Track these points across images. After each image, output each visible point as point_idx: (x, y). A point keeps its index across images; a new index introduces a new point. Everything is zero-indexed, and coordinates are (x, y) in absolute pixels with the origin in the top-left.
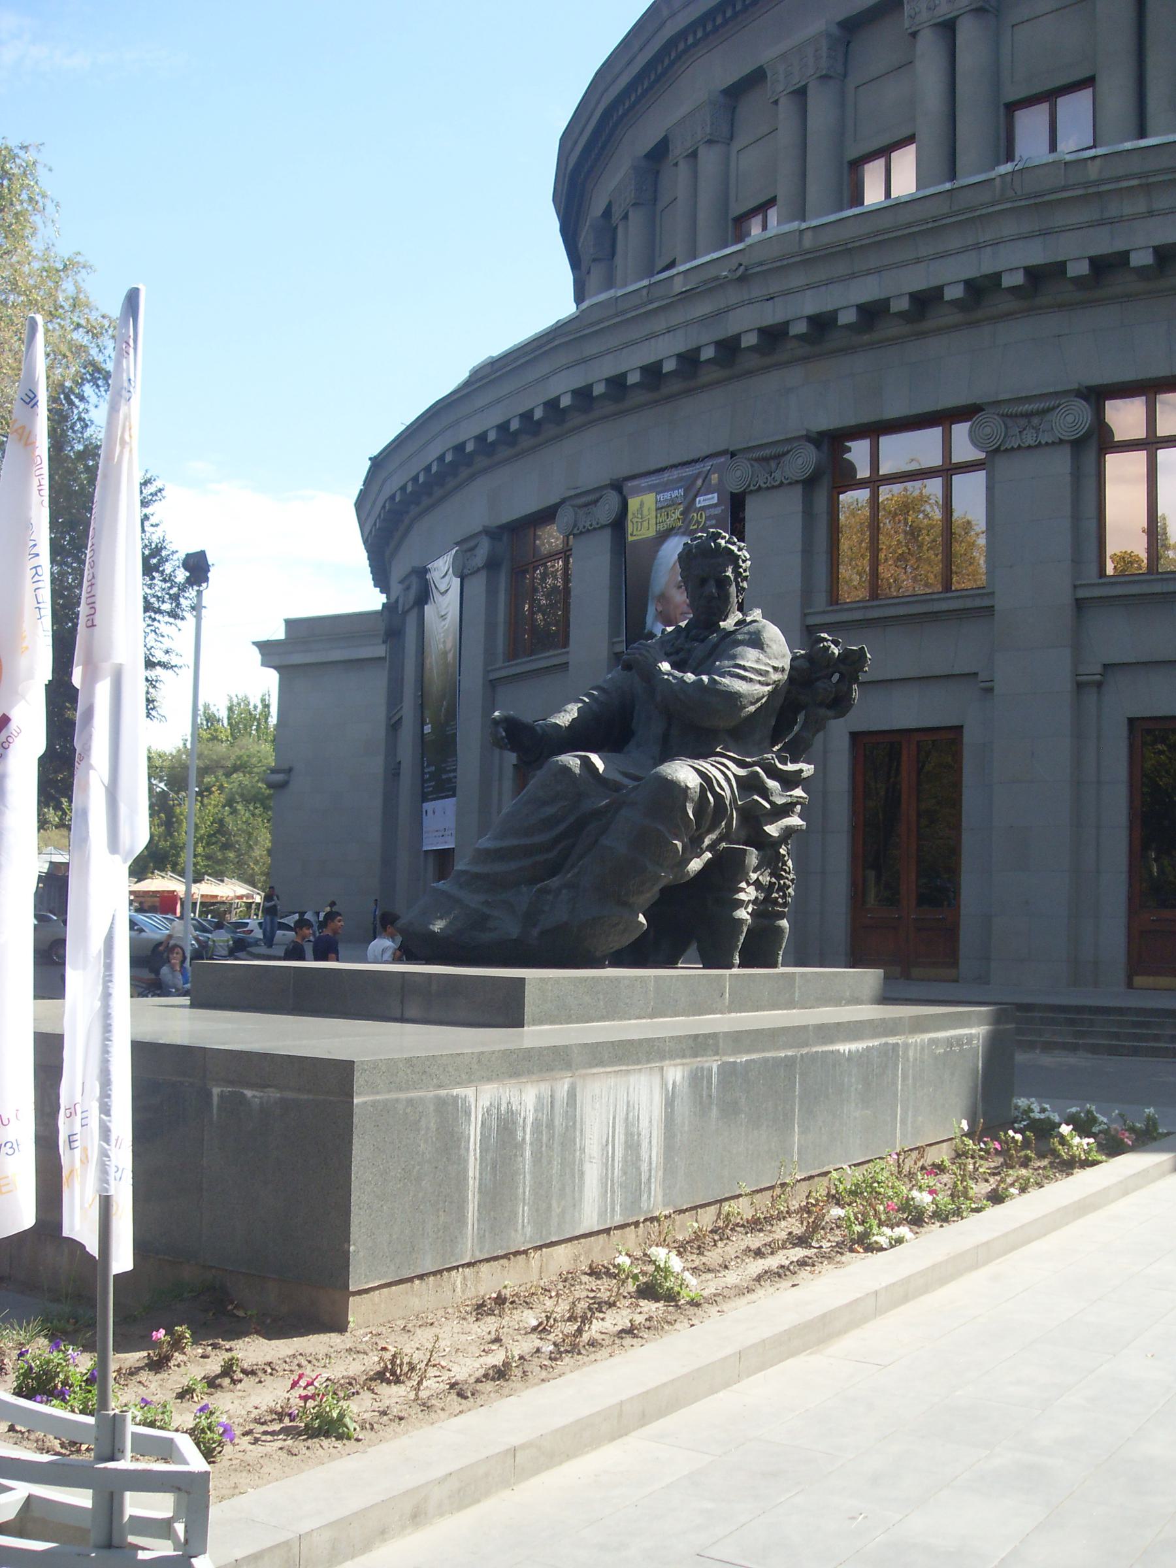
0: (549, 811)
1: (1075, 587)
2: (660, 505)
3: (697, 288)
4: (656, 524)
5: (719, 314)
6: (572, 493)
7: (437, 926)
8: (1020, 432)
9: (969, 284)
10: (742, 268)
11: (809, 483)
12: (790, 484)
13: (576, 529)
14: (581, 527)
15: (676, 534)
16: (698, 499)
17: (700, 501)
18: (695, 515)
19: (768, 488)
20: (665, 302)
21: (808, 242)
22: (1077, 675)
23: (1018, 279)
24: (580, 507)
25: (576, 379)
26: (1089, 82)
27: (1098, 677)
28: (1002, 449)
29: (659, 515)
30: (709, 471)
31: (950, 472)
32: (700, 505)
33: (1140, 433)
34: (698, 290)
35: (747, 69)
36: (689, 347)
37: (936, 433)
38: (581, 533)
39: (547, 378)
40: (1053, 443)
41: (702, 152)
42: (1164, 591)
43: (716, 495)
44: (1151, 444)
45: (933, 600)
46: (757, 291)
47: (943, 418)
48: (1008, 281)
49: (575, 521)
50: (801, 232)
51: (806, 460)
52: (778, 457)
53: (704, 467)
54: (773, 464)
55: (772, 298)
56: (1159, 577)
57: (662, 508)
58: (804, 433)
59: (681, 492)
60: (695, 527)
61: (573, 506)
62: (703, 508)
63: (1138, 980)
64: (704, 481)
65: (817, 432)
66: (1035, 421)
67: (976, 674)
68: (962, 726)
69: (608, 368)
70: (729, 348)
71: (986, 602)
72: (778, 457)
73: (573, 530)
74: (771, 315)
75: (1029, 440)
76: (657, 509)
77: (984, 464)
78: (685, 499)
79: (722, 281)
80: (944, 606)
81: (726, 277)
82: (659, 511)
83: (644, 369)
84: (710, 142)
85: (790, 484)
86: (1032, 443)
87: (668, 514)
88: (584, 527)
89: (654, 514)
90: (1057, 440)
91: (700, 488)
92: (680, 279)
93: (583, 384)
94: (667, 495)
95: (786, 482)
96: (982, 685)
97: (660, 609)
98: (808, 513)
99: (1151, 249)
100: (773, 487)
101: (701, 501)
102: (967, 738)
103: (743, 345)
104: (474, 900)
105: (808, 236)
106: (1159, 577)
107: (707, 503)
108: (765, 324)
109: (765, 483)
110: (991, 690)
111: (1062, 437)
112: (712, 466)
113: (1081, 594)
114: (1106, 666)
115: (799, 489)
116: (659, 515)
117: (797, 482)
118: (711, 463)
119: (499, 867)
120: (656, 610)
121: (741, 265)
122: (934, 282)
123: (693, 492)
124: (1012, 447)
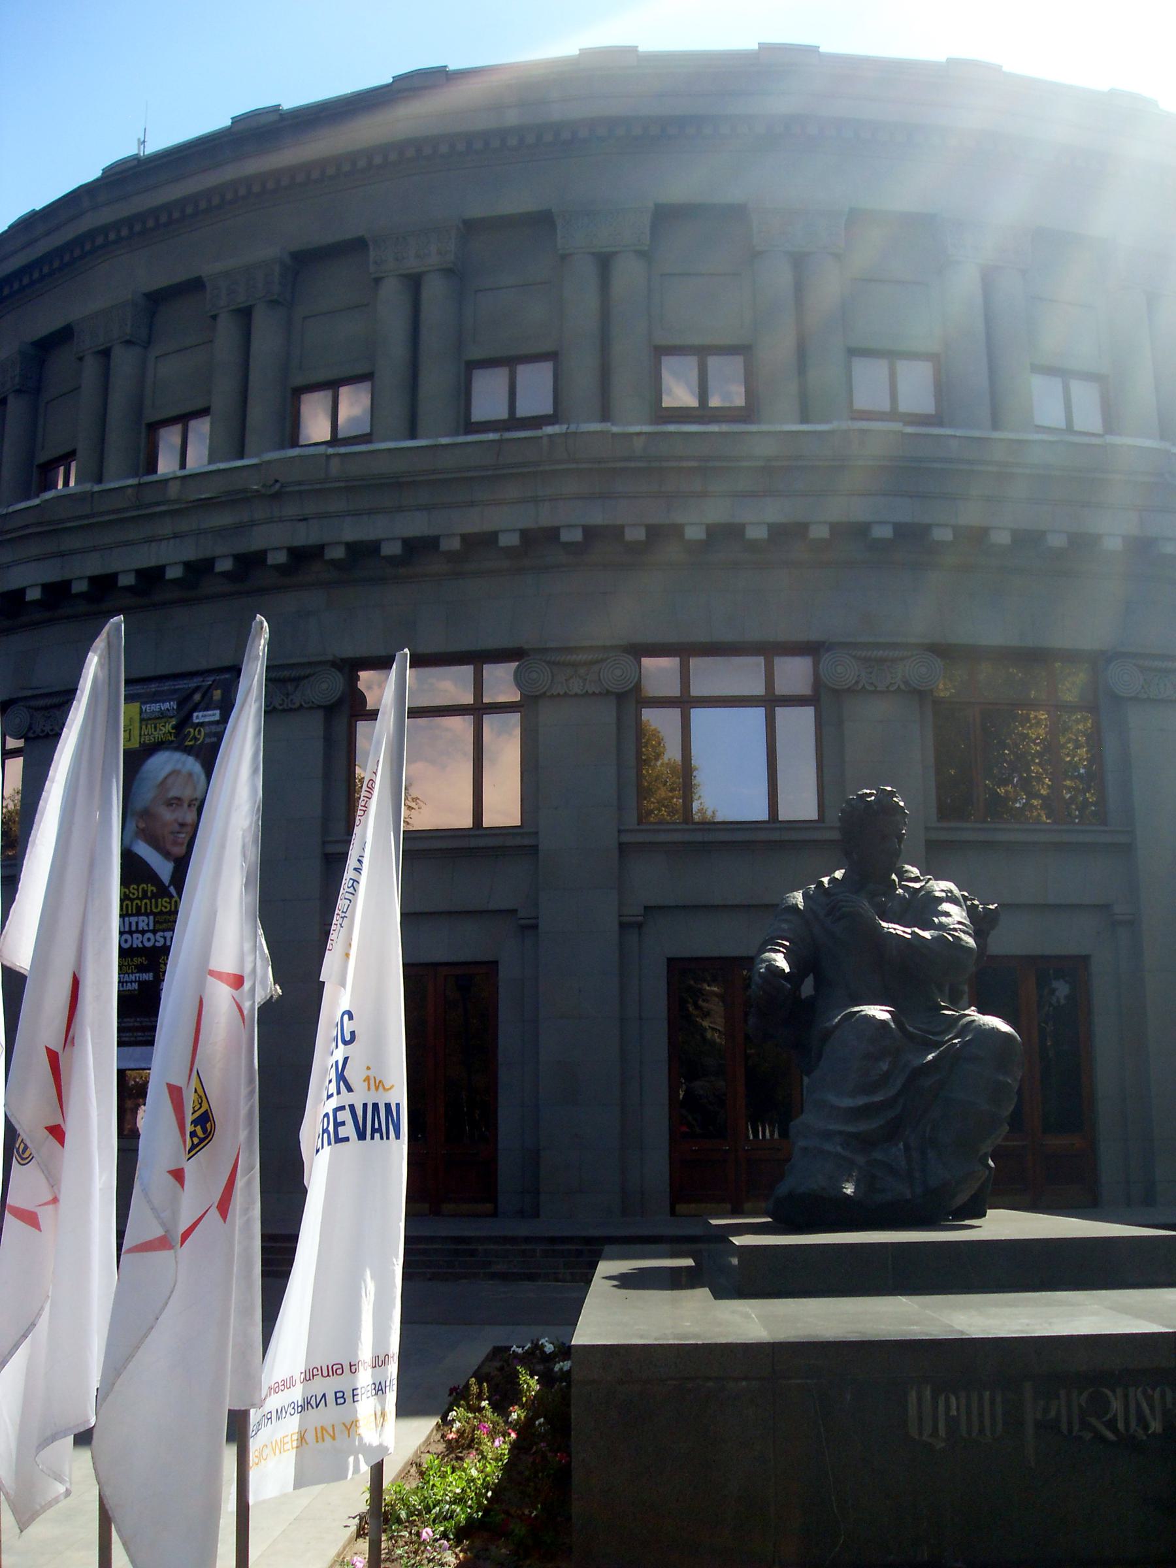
0: (885, 1066)
1: (619, 831)
2: (145, 716)
3: (219, 497)
4: (140, 735)
5: (240, 529)
6: (29, 693)
7: (849, 1190)
8: (566, 680)
9: (525, 534)
10: (277, 486)
11: (330, 711)
12: (311, 708)
13: (32, 731)
14: (38, 730)
15: (167, 749)
16: (195, 714)
17: (197, 717)
18: (192, 730)
19: (284, 710)
20: (177, 506)
21: (335, 467)
22: (620, 916)
23: (577, 536)
24: (37, 709)
25: (50, 573)
26: (551, 356)
27: (640, 918)
28: (548, 694)
29: (144, 727)
30: (211, 685)
31: (481, 712)
32: (197, 721)
33: (674, 691)
34: (219, 500)
35: (180, 276)
36: (201, 556)
37: (466, 671)
38: (38, 737)
39: (8, 567)
40: (600, 694)
41: (118, 352)
42: (706, 839)
43: (218, 712)
44: (685, 703)
45: (469, 836)
46: (291, 509)
47: (478, 658)
48: (565, 536)
49: (31, 724)
50: (328, 457)
51: (329, 686)
52: (297, 680)
53: (203, 681)
54: (290, 687)
55: (305, 519)
56: (694, 827)
57: (150, 719)
58: (330, 658)
59: (174, 705)
60: (191, 743)
61: (29, 707)
62: (201, 724)
63: (681, 1208)
64: (203, 697)
65: (342, 660)
66: (582, 671)
67: (516, 910)
68: (496, 963)
69: (94, 566)
70: (250, 563)
71: (526, 842)
72: (297, 680)
73: (26, 733)
74: (305, 536)
75: (576, 687)
76: (142, 720)
77: (522, 706)
78: (178, 713)
79: (249, 495)
80: (473, 843)
81: (257, 491)
82: (144, 723)
83: (141, 573)
84: (129, 343)
85: (311, 708)
86: (579, 692)
87: (155, 728)
88: (43, 731)
89: (137, 725)
90: (605, 691)
91: (200, 703)
92: (178, 482)
93: (59, 579)
94: (155, 707)
95: (305, 706)
96: (522, 922)
97: (142, 825)
98: (329, 741)
99: (704, 527)
100: (291, 710)
101: (198, 717)
102: (503, 973)
103: (270, 561)
104: (861, 1160)
105: (335, 462)
106: (694, 827)
107: (207, 720)
108: (296, 544)
109: (281, 705)
110: (535, 927)
111: (609, 688)
112: (214, 681)
113: (626, 838)
114: (645, 907)
115: (320, 714)
116: (144, 727)
117: (319, 707)
118: (212, 678)
119: (863, 1126)
120: (137, 827)
121: (277, 481)
122: (488, 527)
123: (190, 705)
124: (559, 694)
